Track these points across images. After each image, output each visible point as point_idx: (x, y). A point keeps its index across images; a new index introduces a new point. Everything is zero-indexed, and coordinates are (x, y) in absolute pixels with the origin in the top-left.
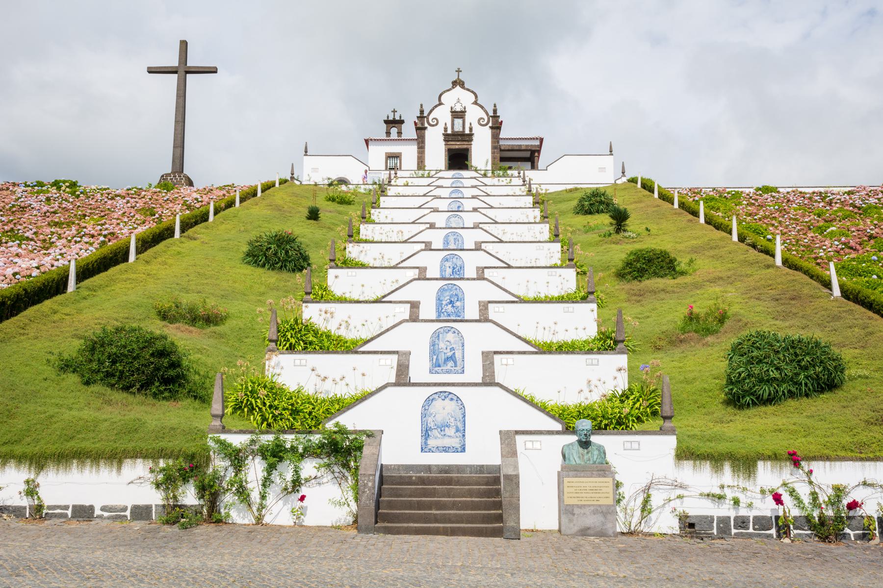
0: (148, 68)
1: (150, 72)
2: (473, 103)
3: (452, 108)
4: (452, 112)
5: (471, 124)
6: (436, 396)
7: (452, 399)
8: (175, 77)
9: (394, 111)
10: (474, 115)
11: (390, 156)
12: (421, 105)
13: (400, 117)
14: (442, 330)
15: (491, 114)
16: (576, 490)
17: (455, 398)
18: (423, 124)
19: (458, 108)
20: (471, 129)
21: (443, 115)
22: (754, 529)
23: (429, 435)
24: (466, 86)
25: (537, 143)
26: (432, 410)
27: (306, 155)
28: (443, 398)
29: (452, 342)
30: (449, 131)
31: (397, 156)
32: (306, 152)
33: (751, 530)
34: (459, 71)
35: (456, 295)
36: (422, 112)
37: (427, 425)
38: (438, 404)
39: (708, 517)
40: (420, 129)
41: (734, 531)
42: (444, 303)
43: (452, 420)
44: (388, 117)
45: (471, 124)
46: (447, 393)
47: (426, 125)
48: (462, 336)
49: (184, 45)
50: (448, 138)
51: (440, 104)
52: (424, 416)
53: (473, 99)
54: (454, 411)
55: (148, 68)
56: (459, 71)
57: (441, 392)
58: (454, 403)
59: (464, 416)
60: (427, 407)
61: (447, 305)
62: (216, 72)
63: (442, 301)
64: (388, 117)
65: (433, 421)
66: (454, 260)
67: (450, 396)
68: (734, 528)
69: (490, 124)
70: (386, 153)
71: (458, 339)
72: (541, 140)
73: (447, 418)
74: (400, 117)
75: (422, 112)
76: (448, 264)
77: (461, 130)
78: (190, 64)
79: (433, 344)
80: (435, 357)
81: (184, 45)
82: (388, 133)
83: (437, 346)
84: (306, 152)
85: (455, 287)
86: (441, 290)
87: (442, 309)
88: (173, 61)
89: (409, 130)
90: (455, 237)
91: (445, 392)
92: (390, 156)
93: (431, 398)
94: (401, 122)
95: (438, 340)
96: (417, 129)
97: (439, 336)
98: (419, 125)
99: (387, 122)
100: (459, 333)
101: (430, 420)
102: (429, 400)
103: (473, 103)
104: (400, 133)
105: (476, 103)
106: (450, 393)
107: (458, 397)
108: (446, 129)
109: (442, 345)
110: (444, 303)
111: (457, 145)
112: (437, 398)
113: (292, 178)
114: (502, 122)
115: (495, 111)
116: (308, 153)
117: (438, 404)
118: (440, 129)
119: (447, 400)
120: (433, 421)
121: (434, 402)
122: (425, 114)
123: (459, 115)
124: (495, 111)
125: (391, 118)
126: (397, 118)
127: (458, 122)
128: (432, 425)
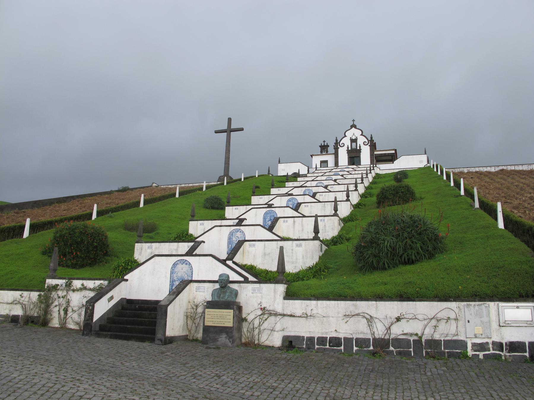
0: (215, 131)
1: (216, 133)
2: (361, 135)
3: (351, 138)
4: (350, 140)
5: (360, 145)
6: (179, 262)
7: (186, 264)
8: (225, 134)
9: (324, 142)
10: (361, 140)
11: (322, 162)
12: (336, 138)
13: (327, 144)
14: (234, 231)
15: (369, 139)
16: (226, 317)
17: (188, 264)
18: (337, 146)
19: (354, 138)
20: (360, 147)
21: (346, 142)
22: (330, 346)
23: (173, 284)
24: (357, 127)
25: (394, 152)
26: (176, 270)
27: (279, 163)
28: (182, 263)
29: (239, 237)
30: (350, 149)
31: (326, 162)
32: (279, 161)
33: (328, 347)
34: (354, 121)
35: (273, 216)
36: (337, 140)
37: (173, 278)
38: (180, 266)
39: (300, 337)
40: (336, 149)
41: (316, 346)
42: (267, 220)
43: (186, 275)
44: (321, 144)
45: (360, 145)
46: (184, 260)
47: (339, 146)
48: (244, 234)
49: (230, 120)
50: (349, 152)
51: (345, 136)
52: (172, 273)
53: (361, 133)
54: (187, 271)
55: (215, 131)
56: (354, 121)
57: (181, 260)
58: (187, 266)
59: (192, 274)
60: (174, 268)
61: (268, 221)
62: (243, 130)
63: (266, 219)
64: (321, 144)
65: (176, 276)
66: (294, 201)
67: (186, 262)
68: (317, 345)
69: (369, 144)
70: (321, 161)
71: (242, 235)
72: (396, 150)
73: (184, 275)
74: (327, 144)
75: (337, 140)
76: (290, 203)
77: (355, 147)
78: (233, 127)
79: (230, 239)
80: (230, 246)
81: (230, 120)
82: (321, 152)
83: (231, 239)
84: (279, 161)
85: (273, 212)
86: (266, 214)
87: (266, 223)
88: (225, 127)
89: (331, 149)
90: (309, 191)
91: (184, 260)
92: (322, 162)
93: (176, 263)
94: (328, 146)
95: (232, 236)
96: (334, 148)
97: (233, 234)
98: (335, 147)
99: (321, 146)
100: (243, 232)
101: (175, 275)
102: (175, 265)
103: (361, 135)
104: (327, 152)
105: (362, 135)
106: (186, 260)
107: (190, 263)
108: (348, 148)
109: (234, 239)
110: (267, 220)
111: (353, 155)
112: (179, 263)
113: (269, 173)
114: (375, 143)
115: (371, 138)
116: (280, 163)
117: (180, 266)
118: (345, 148)
119: (184, 265)
120: (176, 276)
121: (178, 266)
122: (338, 142)
123: (354, 141)
124: (371, 138)
125: (323, 145)
126: (326, 144)
127: (354, 144)
128: (175, 278)
